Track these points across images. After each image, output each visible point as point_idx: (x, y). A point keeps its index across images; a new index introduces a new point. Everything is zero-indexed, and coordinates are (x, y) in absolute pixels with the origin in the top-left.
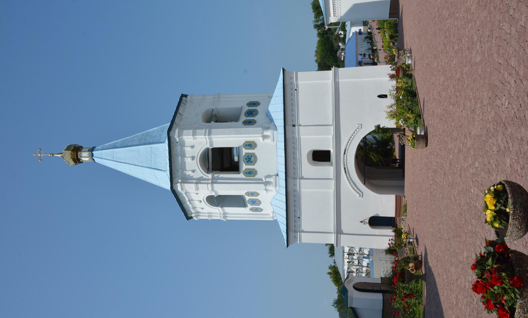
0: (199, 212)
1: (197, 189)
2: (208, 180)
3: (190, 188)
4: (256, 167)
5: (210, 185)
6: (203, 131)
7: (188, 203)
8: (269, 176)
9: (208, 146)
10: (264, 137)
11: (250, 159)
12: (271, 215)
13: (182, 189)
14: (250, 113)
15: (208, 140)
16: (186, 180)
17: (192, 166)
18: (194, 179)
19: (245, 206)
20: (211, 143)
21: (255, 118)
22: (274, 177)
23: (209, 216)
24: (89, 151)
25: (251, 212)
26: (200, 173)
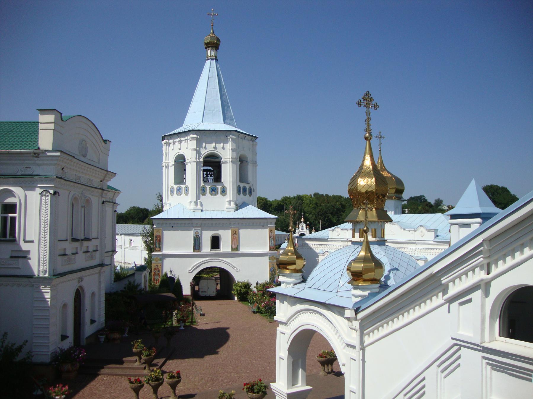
0: (169, 145)
1: (192, 150)
2: (199, 159)
3: (193, 144)
4: (208, 195)
5: (195, 160)
6: (235, 157)
7: (179, 139)
8: (202, 205)
9: (223, 160)
10: (230, 202)
11: (214, 191)
12: (168, 202)
13: (192, 138)
14: (245, 189)
15: (228, 160)
16: (199, 143)
17: (209, 148)
18: (200, 149)
19: (175, 183)
20: (225, 162)
21: (242, 194)
22: (201, 208)
23: (166, 153)
24: (215, 56)
25: (170, 187)
26: (204, 152)
